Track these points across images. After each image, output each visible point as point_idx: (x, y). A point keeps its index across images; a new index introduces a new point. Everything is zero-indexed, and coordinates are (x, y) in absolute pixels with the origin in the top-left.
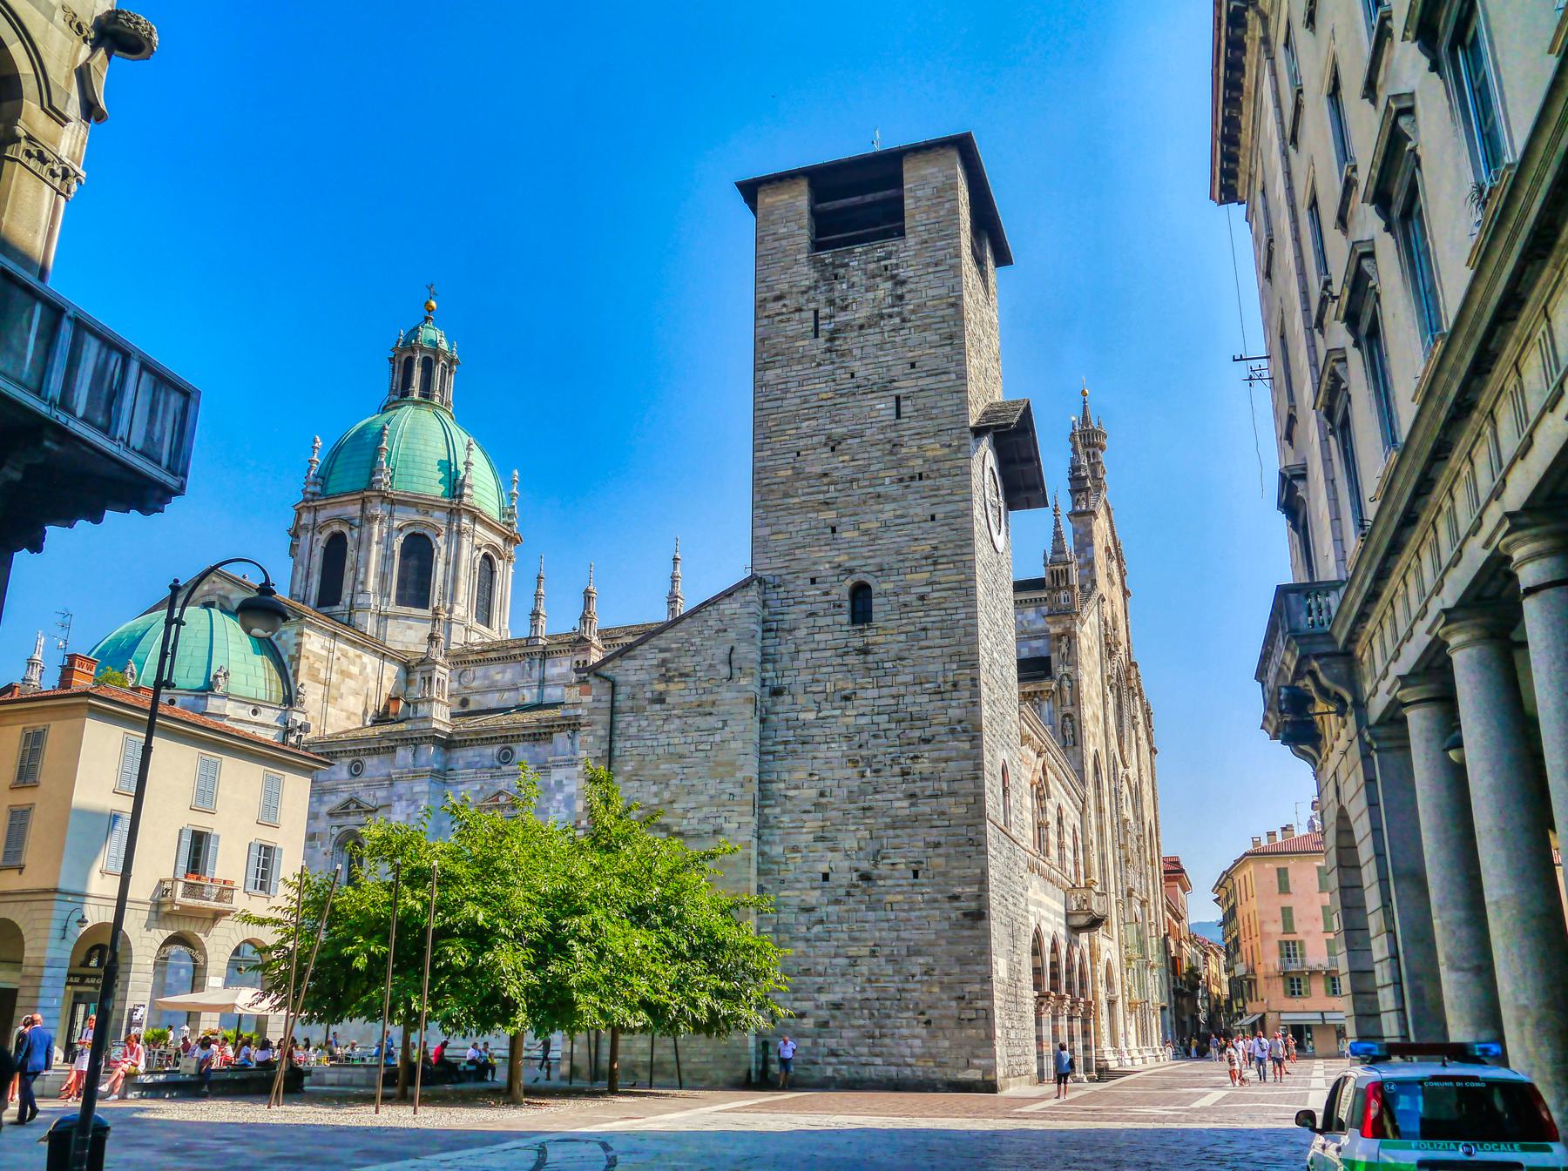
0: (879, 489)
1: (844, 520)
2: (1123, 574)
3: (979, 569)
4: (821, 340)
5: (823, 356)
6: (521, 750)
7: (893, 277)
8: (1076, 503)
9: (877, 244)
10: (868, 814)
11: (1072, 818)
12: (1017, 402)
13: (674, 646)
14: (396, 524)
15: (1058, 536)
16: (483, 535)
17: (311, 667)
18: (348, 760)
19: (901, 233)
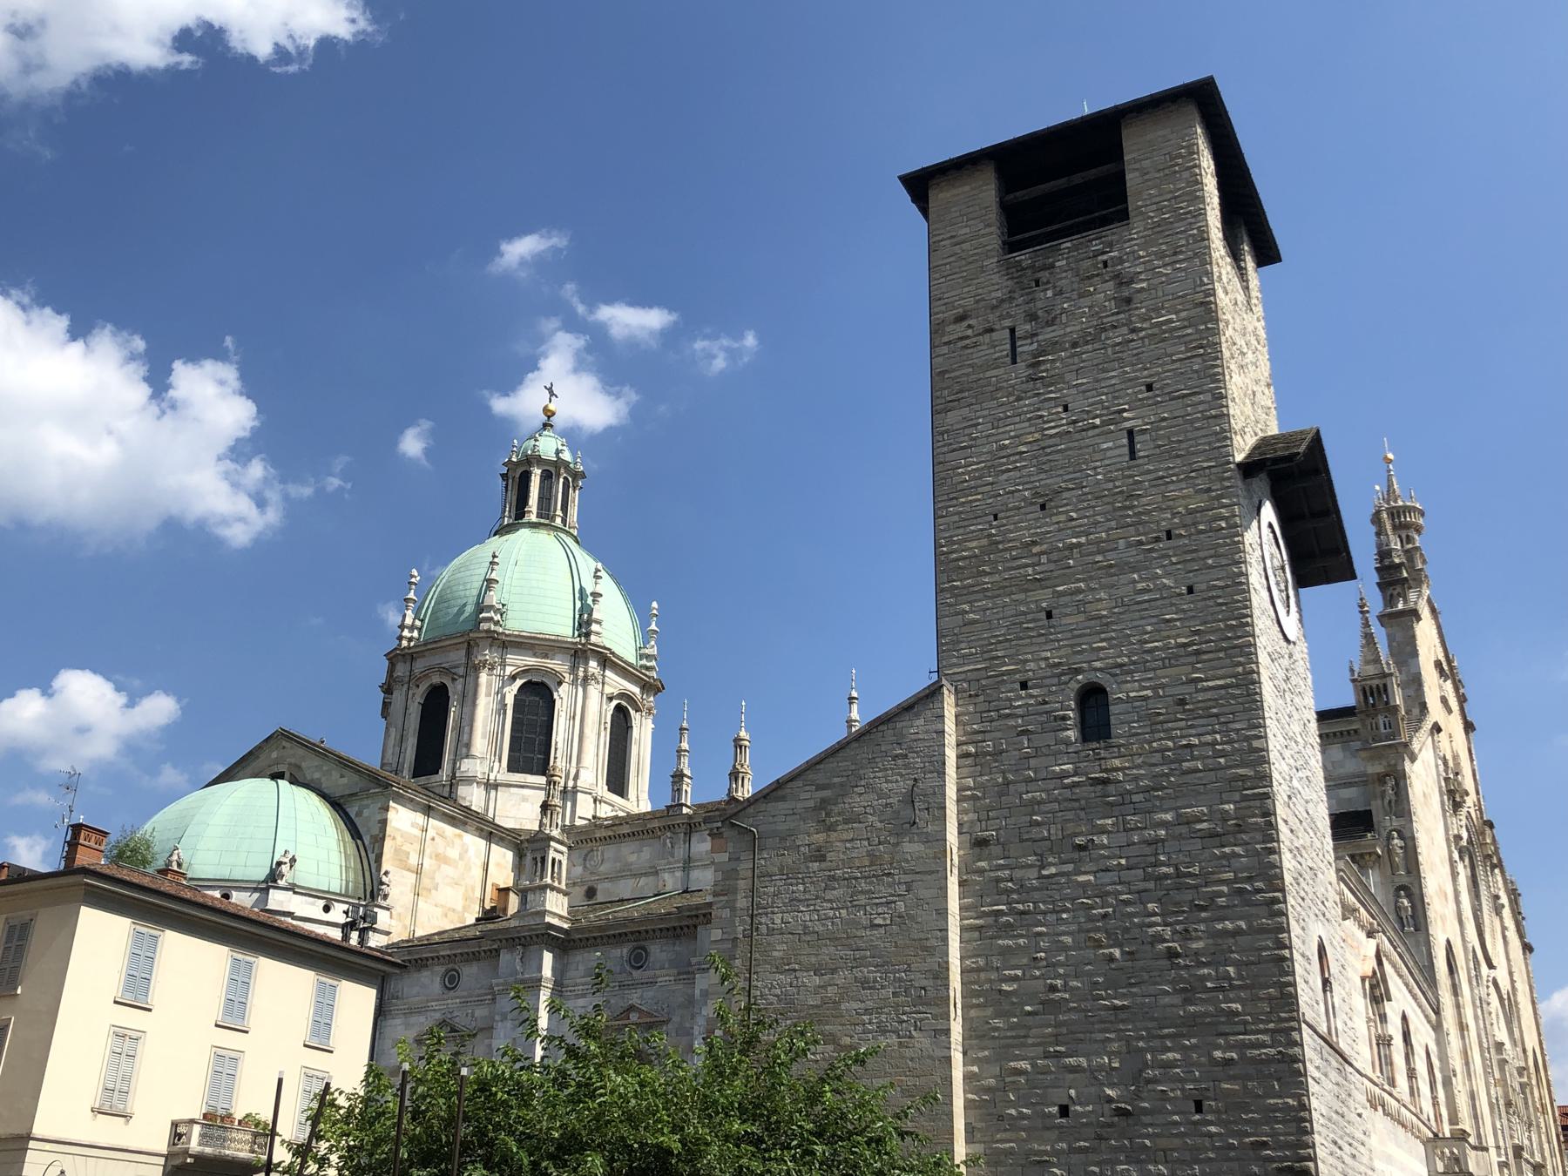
0: (1110, 555)
1: (1063, 600)
2: (1462, 700)
3: (1263, 658)
4: (1021, 365)
5: (1024, 386)
6: (658, 952)
7: (1117, 276)
8: (1390, 601)
9: (1092, 234)
10: (1122, 1016)
11: (1423, 1035)
12: (1302, 432)
13: (836, 780)
14: (509, 670)
15: (1369, 638)
16: (616, 683)
17: (397, 850)
18: (441, 970)
19: (1123, 216)
